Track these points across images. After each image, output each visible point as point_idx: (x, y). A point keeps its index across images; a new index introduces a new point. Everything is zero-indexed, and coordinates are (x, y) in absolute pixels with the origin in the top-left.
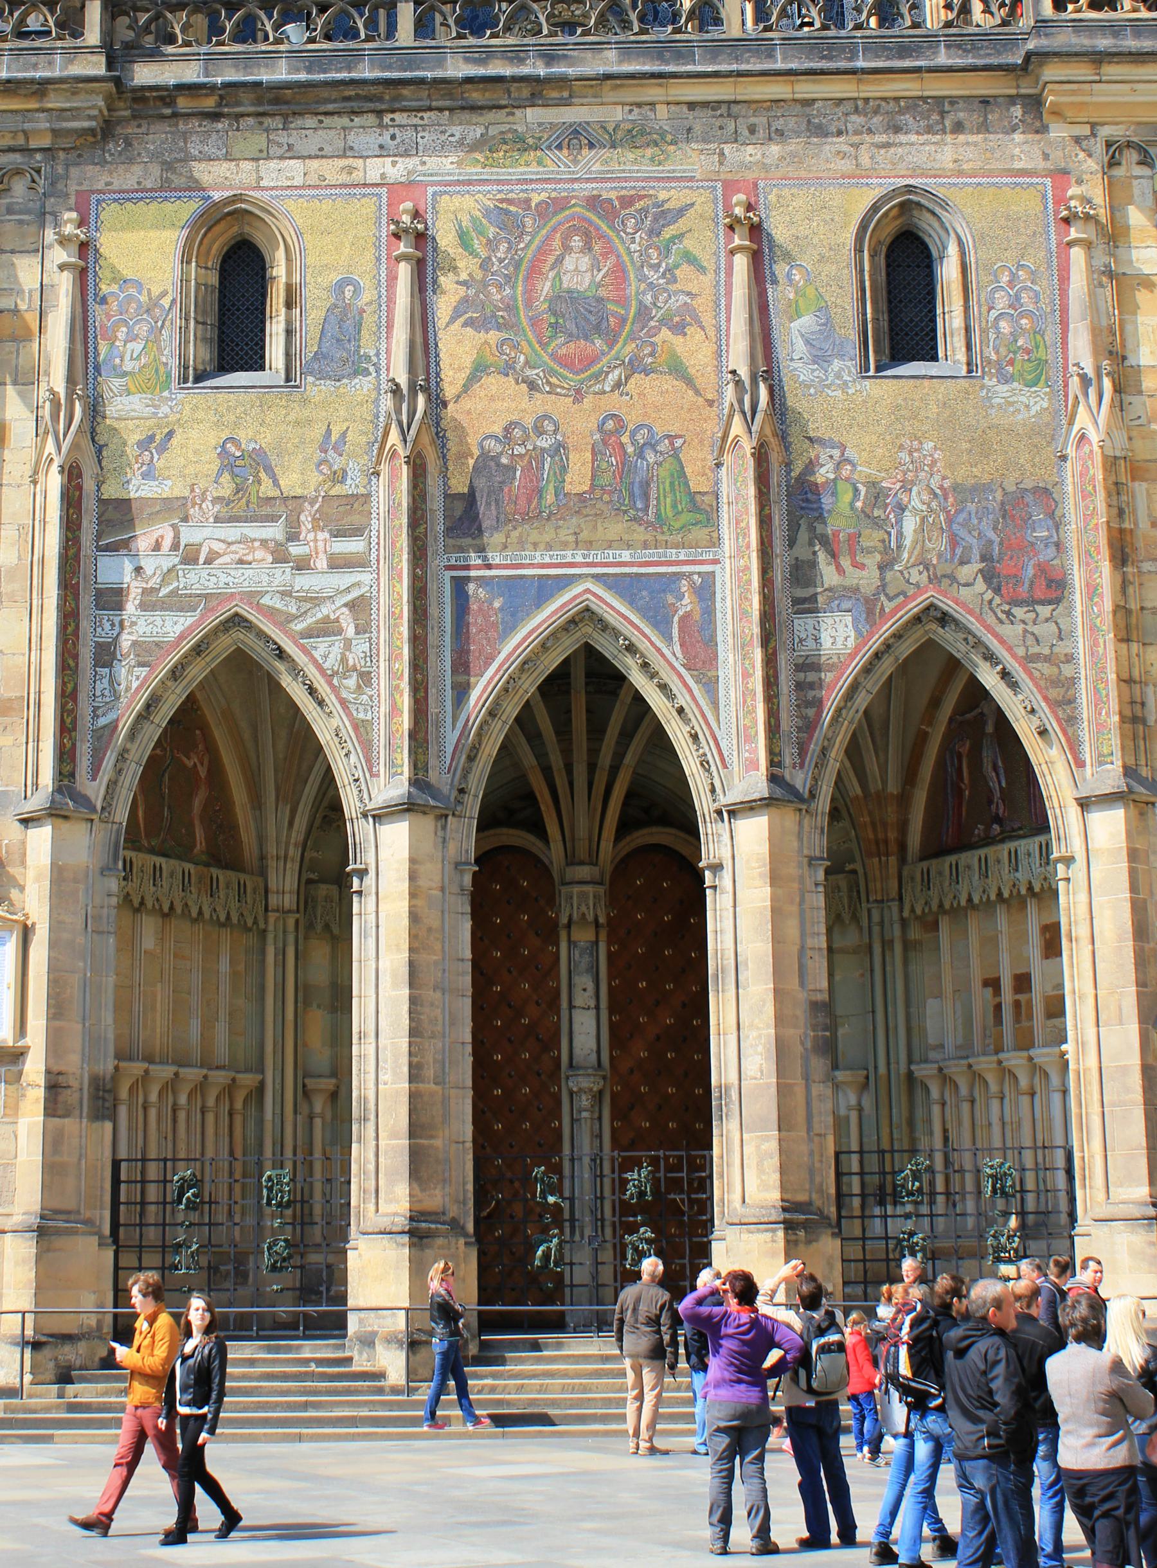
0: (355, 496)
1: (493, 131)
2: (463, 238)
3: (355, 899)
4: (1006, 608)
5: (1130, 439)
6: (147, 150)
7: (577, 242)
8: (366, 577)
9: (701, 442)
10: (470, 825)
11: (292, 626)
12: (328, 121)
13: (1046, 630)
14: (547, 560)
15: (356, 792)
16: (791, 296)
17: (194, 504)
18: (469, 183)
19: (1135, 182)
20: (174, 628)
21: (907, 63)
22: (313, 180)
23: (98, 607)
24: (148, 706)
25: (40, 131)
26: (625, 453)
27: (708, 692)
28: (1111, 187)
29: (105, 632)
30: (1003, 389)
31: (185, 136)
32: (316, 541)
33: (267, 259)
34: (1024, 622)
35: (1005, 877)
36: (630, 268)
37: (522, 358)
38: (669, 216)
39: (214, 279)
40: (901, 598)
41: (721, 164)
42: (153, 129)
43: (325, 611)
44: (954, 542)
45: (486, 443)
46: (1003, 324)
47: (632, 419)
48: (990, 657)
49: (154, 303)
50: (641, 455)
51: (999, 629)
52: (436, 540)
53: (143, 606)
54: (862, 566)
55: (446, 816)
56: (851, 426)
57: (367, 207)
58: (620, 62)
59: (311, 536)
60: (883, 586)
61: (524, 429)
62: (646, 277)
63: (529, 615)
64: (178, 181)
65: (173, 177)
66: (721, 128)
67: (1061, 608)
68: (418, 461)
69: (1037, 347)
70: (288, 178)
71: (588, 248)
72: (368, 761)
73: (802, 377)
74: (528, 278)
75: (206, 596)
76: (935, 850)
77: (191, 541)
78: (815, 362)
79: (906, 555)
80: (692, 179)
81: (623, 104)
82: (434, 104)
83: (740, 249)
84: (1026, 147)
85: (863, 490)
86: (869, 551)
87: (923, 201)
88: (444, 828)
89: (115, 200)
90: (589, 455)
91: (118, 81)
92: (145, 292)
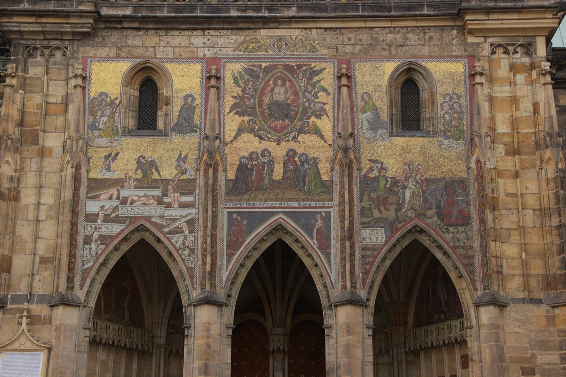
0: (190, 180)
1: (248, 38)
3: (186, 339)
4: (446, 227)
5: (497, 161)
6: (111, 42)
7: (279, 82)
8: (193, 211)
9: (326, 161)
10: (232, 309)
11: (164, 230)
12: (183, 32)
13: (462, 236)
14: (265, 206)
15: (187, 296)
16: (363, 104)
17: (126, 181)
18: (238, 58)
19: (502, 60)
20: (116, 229)
21: (411, 13)
22: (177, 55)
23: (86, 221)
24: (105, 261)
26: (297, 165)
27: (327, 258)
28: (490, 62)
29: (89, 231)
30: (446, 141)
31: (126, 37)
32: (174, 196)
34: (453, 233)
35: (446, 336)
36: (300, 93)
37: (257, 127)
38: (316, 73)
39: (137, 93)
40: (404, 223)
41: (337, 52)
42: (113, 33)
43: (177, 224)
44: (425, 201)
45: (242, 160)
46: (447, 116)
47: (300, 151)
48: (440, 247)
49: (113, 102)
50: (302, 165)
51: (443, 235)
52: (221, 197)
53: (105, 221)
54: (389, 210)
55: (222, 306)
56: (385, 155)
57: (198, 67)
58: (298, 12)
59: (172, 195)
60: (397, 219)
61: (257, 155)
63: (257, 226)
64: (123, 54)
65: (121, 53)
66: (337, 38)
67: (468, 228)
68: (215, 166)
69: (460, 125)
70: (167, 55)
71: (284, 85)
72: (192, 283)
73: (367, 136)
74: (261, 97)
75: (129, 217)
76: (418, 324)
77: (125, 196)
78: (371, 130)
79: (406, 206)
80: (325, 58)
81: (299, 28)
82: (225, 27)
84: (457, 47)
85: (390, 180)
86: (391, 204)
88: (221, 310)
89: (97, 61)
90: (282, 165)
91: (98, 13)
92: (109, 98)
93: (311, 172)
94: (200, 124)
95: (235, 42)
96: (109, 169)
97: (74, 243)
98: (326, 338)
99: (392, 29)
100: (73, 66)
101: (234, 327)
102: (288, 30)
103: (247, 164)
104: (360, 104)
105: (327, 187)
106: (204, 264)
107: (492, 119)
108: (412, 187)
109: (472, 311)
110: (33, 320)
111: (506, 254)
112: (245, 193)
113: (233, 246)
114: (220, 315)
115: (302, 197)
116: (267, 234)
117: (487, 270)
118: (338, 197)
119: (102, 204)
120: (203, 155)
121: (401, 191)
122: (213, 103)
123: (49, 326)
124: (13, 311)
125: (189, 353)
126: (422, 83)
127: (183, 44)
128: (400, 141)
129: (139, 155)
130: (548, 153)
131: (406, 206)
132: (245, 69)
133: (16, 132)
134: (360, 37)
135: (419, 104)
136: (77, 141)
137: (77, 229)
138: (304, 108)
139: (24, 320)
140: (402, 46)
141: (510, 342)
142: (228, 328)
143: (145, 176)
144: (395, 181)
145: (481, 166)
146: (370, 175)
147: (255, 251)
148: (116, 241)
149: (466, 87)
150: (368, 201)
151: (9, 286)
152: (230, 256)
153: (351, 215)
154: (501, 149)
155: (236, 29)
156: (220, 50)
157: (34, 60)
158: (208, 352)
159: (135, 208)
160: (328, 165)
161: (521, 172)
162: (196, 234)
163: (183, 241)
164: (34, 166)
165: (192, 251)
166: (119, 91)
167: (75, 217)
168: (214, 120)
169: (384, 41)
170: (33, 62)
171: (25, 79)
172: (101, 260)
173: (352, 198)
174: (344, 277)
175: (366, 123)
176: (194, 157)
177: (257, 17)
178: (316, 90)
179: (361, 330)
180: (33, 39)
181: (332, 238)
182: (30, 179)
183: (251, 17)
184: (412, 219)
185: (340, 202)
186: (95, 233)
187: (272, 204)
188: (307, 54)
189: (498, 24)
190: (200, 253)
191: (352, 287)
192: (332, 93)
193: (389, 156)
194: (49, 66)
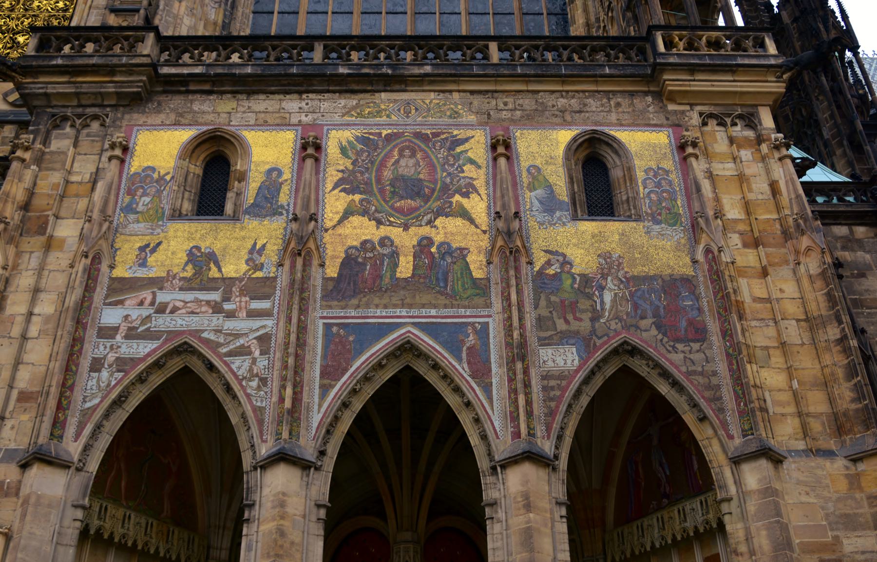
0: (267, 278)
2: (343, 151)
3: (245, 525)
4: (672, 344)
6: (169, 108)
7: (407, 152)
8: (269, 323)
9: (480, 252)
10: (326, 476)
12: (271, 96)
14: (384, 314)
15: (251, 454)
18: (348, 125)
19: (717, 133)
20: (143, 349)
22: (261, 122)
23: (99, 337)
24: (120, 396)
25: (109, 93)
26: (434, 257)
29: (100, 352)
31: (192, 102)
32: (240, 302)
33: (232, 162)
34: (683, 352)
37: (373, 208)
39: (199, 171)
40: (606, 338)
41: (489, 118)
42: (174, 98)
43: (242, 341)
44: (636, 306)
46: (653, 196)
47: (438, 239)
48: (665, 374)
49: (161, 178)
50: (443, 258)
51: (669, 356)
52: (315, 301)
53: (127, 337)
54: (580, 320)
55: (310, 467)
59: (238, 299)
60: (593, 332)
61: (373, 244)
64: (183, 121)
65: (182, 119)
68: (308, 258)
69: (674, 207)
75: (166, 332)
77: (163, 301)
78: (544, 212)
80: (472, 125)
81: (434, 91)
83: (502, 155)
85: (578, 279)
87: (602, 137)
88: (308, 476)
90: (411, 258)
92: (157, 173)
93: (455, 267)
94: (288, 205)
95: (344, 107)
96: (143, 263)
97: (74, 368)
98: (487, 522)
100: (112, 136)
101: (329, 505)
103: (357, 257)
104: (525, 179)
105: (481, 288)
106: (282, 400)
107: (717, 199)
108: (613, 287)
109: (728, 473)
111: (767, 382)
112: (353, 297)
113: (330, 374)
114: (305, 483)
115: (443, 302)
116: (387, 356)
117: (746, 405)
119: (125, 313)
121: (596, 292)
122: (308, 176)
123: (15, 499)
125: (249, 549)
126: (611, 159)
127: (270, 109)
128: (589, 227)
129: (191, 245)
130: (805, 242)
131: (607, 314)
132: (357, 137)
133: (16, 217)
134: (521, 102)
135: (609, 185)
136: (101, 225)
137: (82, 348)
140: (580, 112)
141: (795, 519)
142: (319, 506)
143: (198, 273)
144: (586, 279)
145: (714, 257)
147: (367, 384)
148: (141, 367)
149: (674, 161)
150: (547, 307)
152: (325, 390)
154: (735, 239)
155: (347, 91)
156: (323, 116)
157: (61, 131)
158: (280, 543)
160: (482, 258)
161: (770, 270)
162: (272, 355)
163: (251, 367)
164: (34, 262)
165: (263, 381)
166: (172, 164)
167: (80, 331)
168: (309, 198)
169: (553, 106)
170: (59, 134)
171: (43, 153)
172: (113, 395)
173: (523, 301)
174: (515, 418)
175: (536, 203)
176: (276, 247)
177: (375, 75)
178: (461, 162)
179: (548, 506)
180: (64, 106)
181: (493, 360)
182: (25, 280)
183: (367, 75)
184: (618, 333)
186: (110, 355)
187: (395, 312)
188: (447, 120)
191: (529, 434)
192: (484, 165)
193: (575, 245)
194: (80, 138)
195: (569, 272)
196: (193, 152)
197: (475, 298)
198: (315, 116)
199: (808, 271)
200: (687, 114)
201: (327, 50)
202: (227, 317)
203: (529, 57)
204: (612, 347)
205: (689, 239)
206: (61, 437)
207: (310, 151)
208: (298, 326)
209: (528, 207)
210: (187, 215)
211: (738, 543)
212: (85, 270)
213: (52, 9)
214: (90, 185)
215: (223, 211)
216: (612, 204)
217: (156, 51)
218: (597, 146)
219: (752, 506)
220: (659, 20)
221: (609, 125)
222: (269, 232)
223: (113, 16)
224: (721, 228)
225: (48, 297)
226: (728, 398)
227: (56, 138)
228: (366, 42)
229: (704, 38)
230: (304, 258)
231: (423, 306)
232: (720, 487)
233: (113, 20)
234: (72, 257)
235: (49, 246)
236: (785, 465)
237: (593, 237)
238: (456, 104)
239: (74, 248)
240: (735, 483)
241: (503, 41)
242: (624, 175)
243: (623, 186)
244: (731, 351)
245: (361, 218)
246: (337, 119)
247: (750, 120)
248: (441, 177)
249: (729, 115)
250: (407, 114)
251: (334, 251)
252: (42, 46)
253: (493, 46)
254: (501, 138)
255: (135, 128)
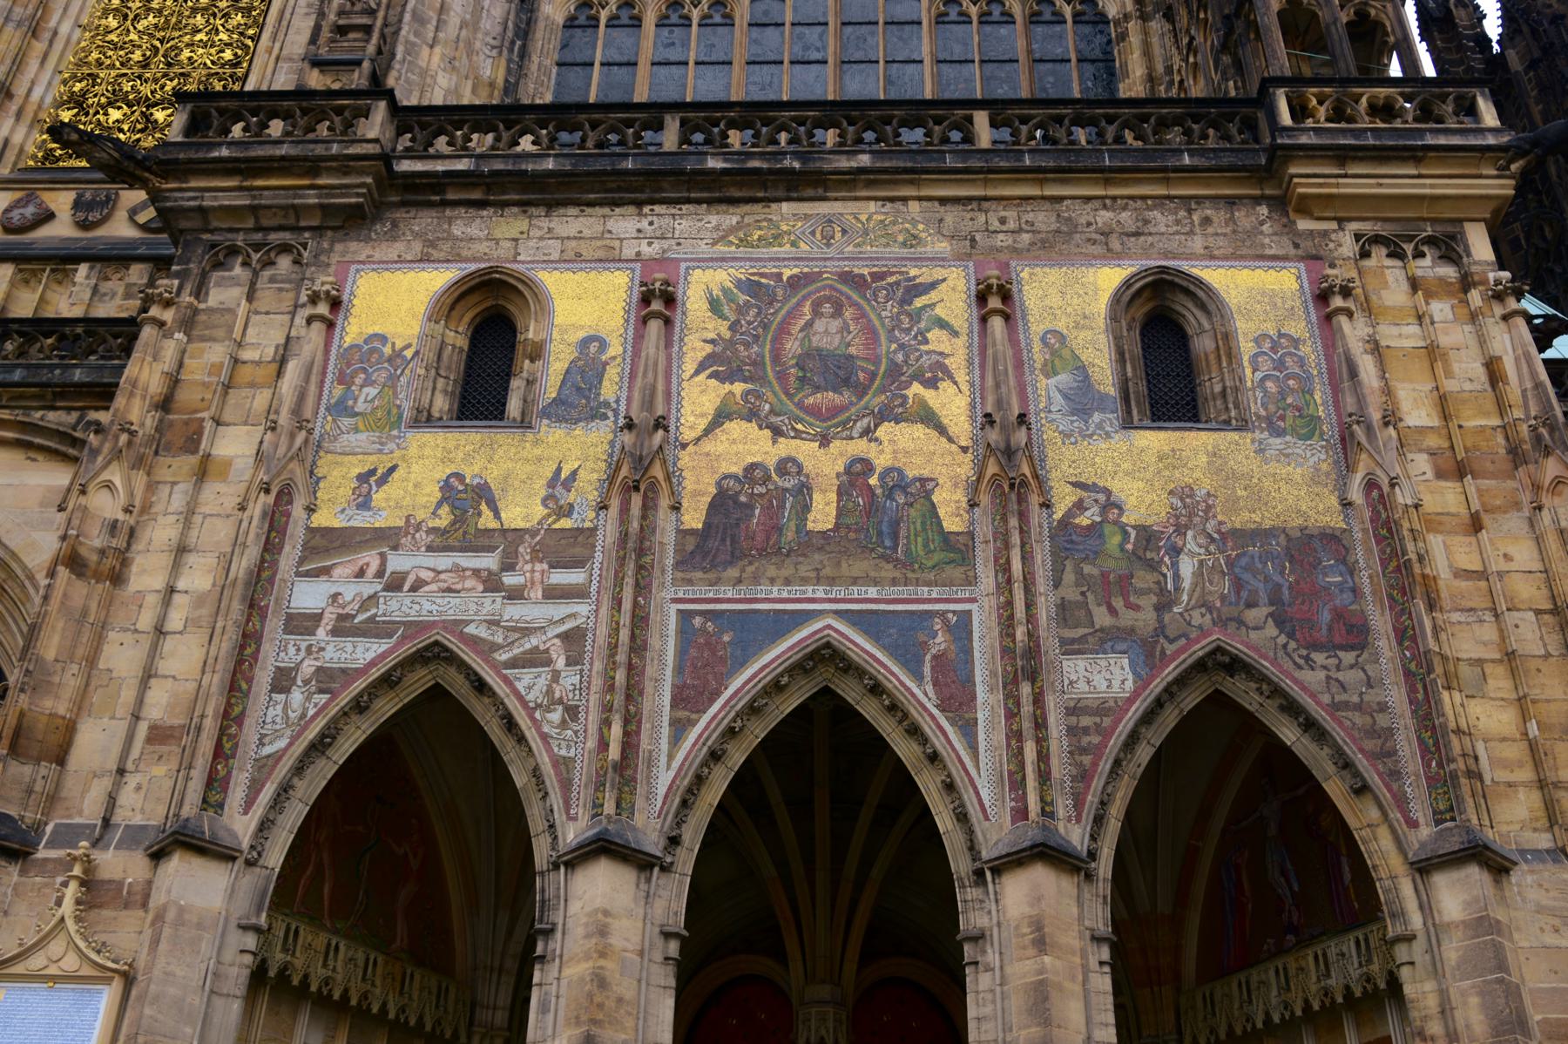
0: (580, 530)
2: (714, 306)
3: (537, 967)
4: (1304, 652)
7: (827, 308)
8: (583, 609)
9: (956, 485)
10: (681, 882)
11: (496, 656)
12: (589, 210)
13: (1349, 677)
14: (785, 595)
15: (549, 840)
18: (723, 260)
19: (1387, 272)
20: (364, 653)
22: (570, 255)
23: (287, 631)
24: (322, 735)
26: (873, 494)
27: (965, 735)
29: (290, 657)
31: (450, 221)
32: (533, 571)
34: (1325, 667)
37: (767, 407)
39: (462, 342)
40: (1183, 641)
41: (972, 247)
42: (420, 214)
44: (1238, 585)
46: (1269, 384)
47: (881, 461)
48: (1292, 708)
49: (397, 354)
50: (890, 497)
51: (1297, 674)
52: (663, 571)
53: (335, 632)
54: (1137, 608)
55: (652, 866)
59: (528, 567)
60: (1160, 630)
62: (895, 340)
63: (761, 649)
64: (435, 254)
68: (650, 494)
69: (1308, 405)
75: (404, 623)
77: (399, 569)
79: (1185, 597)
80: (943, 259)
81: (876, 199)
83: (995, 312)
86: (1141, 593)
88: (648, 881)
90: (833, 497)
92: (389, 345)
93: (913, 512)
94: (617, 401)
95: (717, 228)
96: (365, 504)
97: (244, 686)
99: (1108, 202)
100: (313, 280)
101: (685, 933)
102: (850, 204)
103: (738, 493)
104: (1038, 354)
105: (958, 549)
106: (603, 745)
107: (1388, 391)
108: (1197, 550)
109: (1407, 889)
110: (95, 892)
111: (1481, 725)
112: (731, 563)
113: (688, 700)
114: (643, 894)
115: (890, 575)
117: (1440, 765)
118: (992, 574)
119: (333, 590)
120: (618, 468)
121: (1166, 559)
122: (652, 351)
123: (141, 913)
124: (50, 866)
125: (544, 1009)
126: (1193, 318)
127: (587, 233)
128: (1153, 441)
129: (448, 471)
131: (1185, 597)
132: (739, 280)
133: (149, 422)
134: (1030, 217)
135: (1189, 366)
136: (292, 436)
137: (258, 650)
138: (892, 362)
139: (72, 890)
140: (1137, 234)
141: (1533, 976)
143: (459, 520)
144: (1147, 535)
145: (1382, 496)
146: (1077, 521)
147: (753, 718)
148: (360, 685)
151: (52, 799)
152: (679, 728)
153: (1031, 618)
154: (1421, 464)
155: (720, 201)
158: (598, 999)
159: (423, 601)
160: (961, 497)
161: (1486, 519)
162: (587, 667)
163: (549, 686)
164: (178, 501)
165: (572, 712)
166: (416, 330)
169: (1089, 224)
171: (196, 311)
172: (311, 734)
173: (1033, 574)
174: (1018, 784)
175: (1058, 399)
176: (595, 476)
177: (770, 171)
178: (922, 325)
179: (1077, 944)
180: (231, 230)
181: (978, 679)
182: (162, 532)
184: (1204, 633)
185: (998, 585)
187: (804, 592)
188: (896, 250)
189: (1371, 186)
190: (593, 718)
192: (964, 331)
193: (1127, 474)
194: (259, 285)
195: (1116, 523)
196: (452, 308)
197: (948, 568)
198: (665, 244)
199: (1556, 521)
200: (1333, 236)
201: (687, 128)
202: (509, 598)
203: (1044, 137)
204: (1195, 657)
205: (1336, 462)
206: (221, 806)
207: (656, 305)
208: (634, 616)
209: (1042, 405)
210: (441, 419)
211: (1425, 1018)
212: (264, 514)
213: (213, 63)
214: (275, 366)
215: (503, 412)
216: (1194, 400)
217: (390, 133)
218: (1168, 295)
219: (1452, 952)
220: (1282, 66)
221: (1190, 257)
222: (583, 450)
223: (316, 72)
224: (1394, 443)
225: (202, 560)
226: (1407, 752)
227: (218, 285)
228: (753, 113)
229: (1364, 100)
230: (645, 497)
231: (855, 581)
232: (1393, 916)
233: (316, 80)
234: (242, 492)
235: (202, 473)
236: (1515, 877)
237: (1160, 459)
238: (914, 222)
239: (247, 477)
240: (1421, 907)
241: (999, 110)
242: (1218, 348)
243: (1214, 367)
244: (1413, 666)
245: (744, 424)
246: (703, 249)
247: (1449, 248)
248: (888, 352)
249: (1410, 239)
250: (828, 239)
251: (698, 482)
252: (195, 126)
253: (981, 119)
254: (994, 281)
255: (353, 267)
